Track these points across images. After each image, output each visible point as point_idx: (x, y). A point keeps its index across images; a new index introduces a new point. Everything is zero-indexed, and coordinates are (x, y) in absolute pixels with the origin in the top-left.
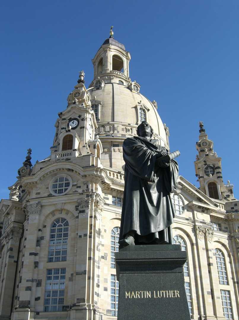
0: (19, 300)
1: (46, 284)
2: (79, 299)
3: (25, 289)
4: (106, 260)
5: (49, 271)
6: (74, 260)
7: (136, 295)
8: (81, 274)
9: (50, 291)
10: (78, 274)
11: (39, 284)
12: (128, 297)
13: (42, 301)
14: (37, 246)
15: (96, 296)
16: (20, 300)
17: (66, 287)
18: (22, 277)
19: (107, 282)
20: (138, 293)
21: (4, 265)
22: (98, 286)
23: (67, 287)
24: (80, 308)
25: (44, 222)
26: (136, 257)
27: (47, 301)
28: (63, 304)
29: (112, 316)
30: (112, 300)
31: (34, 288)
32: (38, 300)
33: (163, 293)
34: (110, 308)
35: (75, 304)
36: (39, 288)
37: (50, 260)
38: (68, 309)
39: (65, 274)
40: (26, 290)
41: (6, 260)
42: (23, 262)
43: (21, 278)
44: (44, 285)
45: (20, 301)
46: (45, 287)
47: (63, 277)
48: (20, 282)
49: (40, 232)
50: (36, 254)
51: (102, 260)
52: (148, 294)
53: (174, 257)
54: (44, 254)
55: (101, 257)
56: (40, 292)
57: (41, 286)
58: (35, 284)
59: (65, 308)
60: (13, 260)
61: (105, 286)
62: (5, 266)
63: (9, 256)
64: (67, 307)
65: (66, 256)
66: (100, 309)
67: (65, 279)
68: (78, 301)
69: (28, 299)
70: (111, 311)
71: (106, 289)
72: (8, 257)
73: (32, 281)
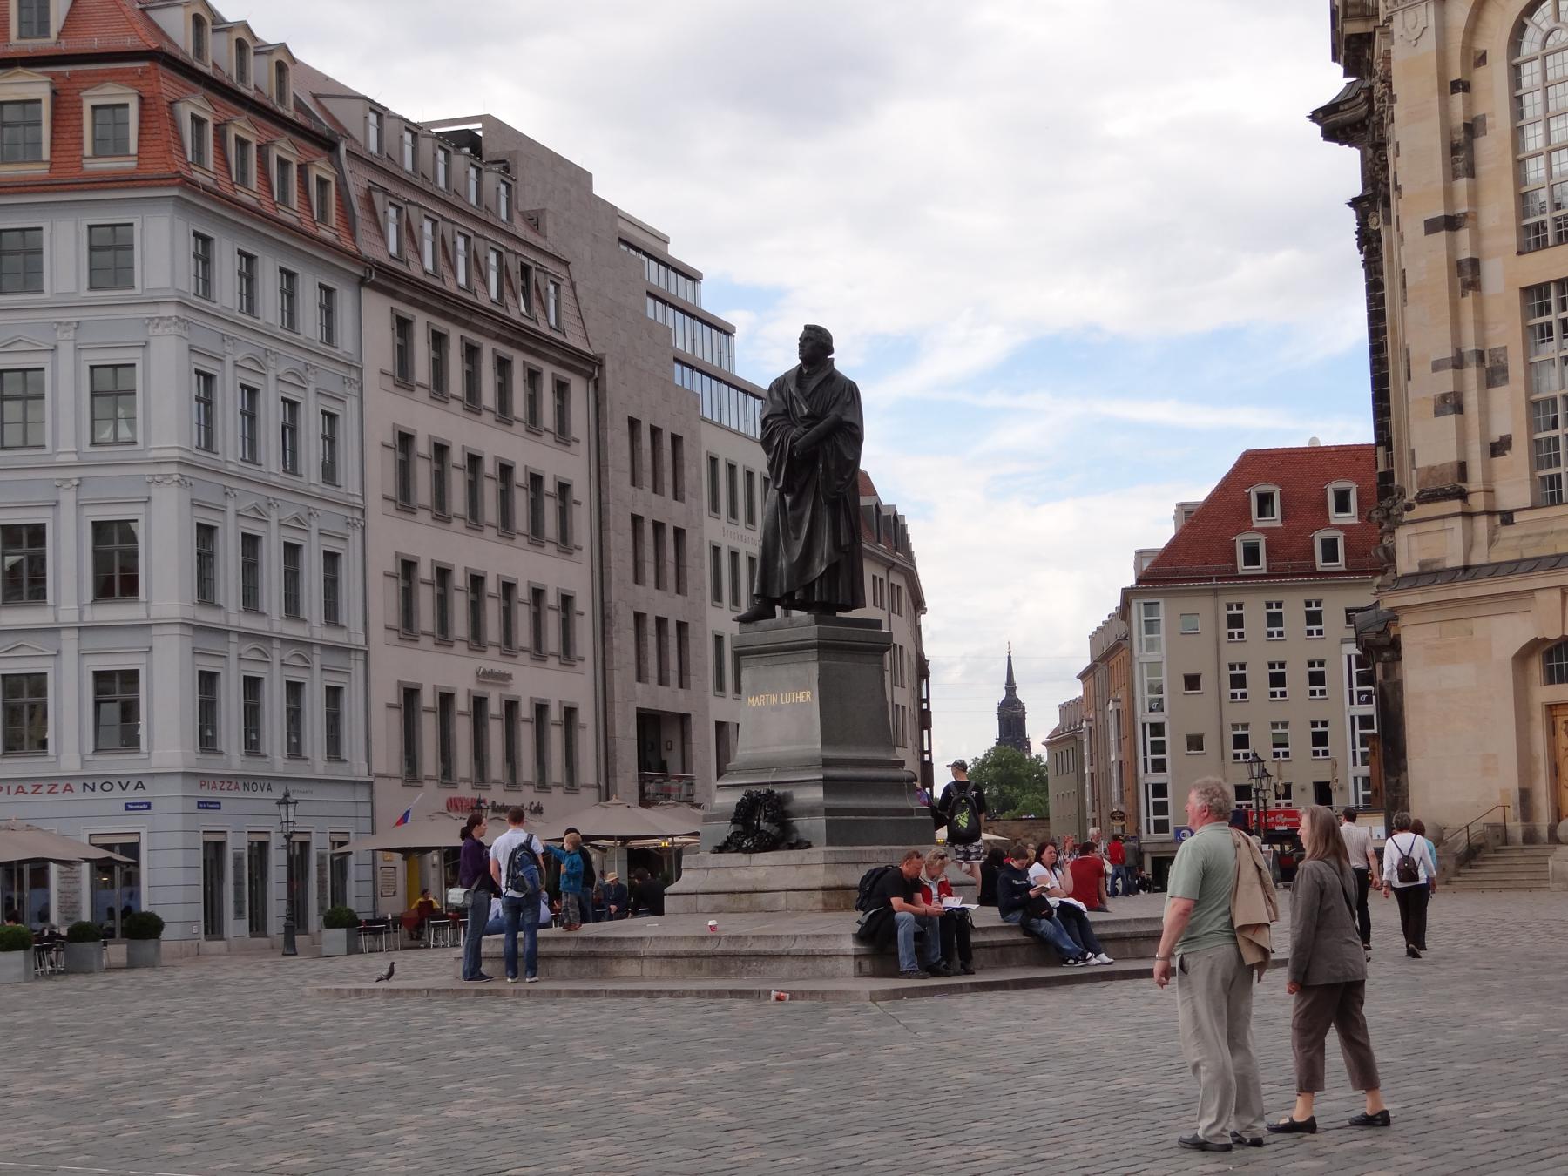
1: (1530, 367)
5: (1535, 295)
9: (1554, 400)
11: (1494, 375)
13: (1520, 453)
14: (1455, 177)
25: (1472, 30)
27: (1545, 453)
31: (1472, 400)
32: (1503, 454)
36: (1499, 395)
37: (1532, 239)
40: (1437, 414)
44: (1521, 372)
45: (1418, 471)
46: (1531, 386)
49: (1459, 96)
50: (1451, 223)
52: (774, 698)
54: (1497, 213)
56: (1506, 411)
57: (1506, 378)
58: (1472, 374)
69: (1452, 457)
73: (1458, 362)
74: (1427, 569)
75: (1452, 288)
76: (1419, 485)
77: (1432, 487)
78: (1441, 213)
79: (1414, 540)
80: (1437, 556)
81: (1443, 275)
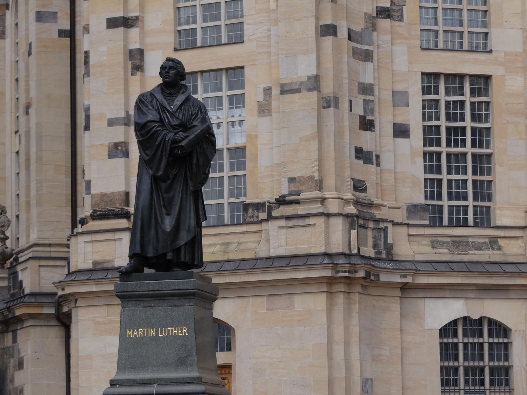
0: (90, 193)
2: (295, 179)
3: (106, 153)
4: (401, 19)
6: (269, 37)
7: (139, 333)
8: (298, 91)
10: (286, 90)
12: (130, 335)
15: (361, 162)
16: (94, 191)
17: (249, 137)
18: (92, 112)
19: (407, 105)
20: (141, 331)
21: (23, 48)
22: (367, 125)
23: (252, 138)
24: (300, 210)
26: (139, 289)
28: (245, 195)
29: (433, 225)
30: (429, 169)
33: (169, 330)
34: (420, 199)
35: (284, 196)
38: (263, 216)
39: (243, 88)
40: (111, 156)
41: (27, 29)
42: (87, 53)
43: (87, 110)
45: (93, 196)
47: (236, 101)
48: (87, 128)
50: (126, 23)
51: (384, 23)
52: (152, 332)
53: (182, 287)
55: (375, 15)
59: (250, 212)
60: (52, 29)
61: (400, 120)
62: (30, 54)
63: (38, 13)
64: (259, 206)
65: (242, 23)
66: (379, 206)
67: (244, 107)
68: (292, 184)
69: (122, 188)
70: (424, 208)
71: (401, 131)
72: (32, 16)
74: (99, 267)
75: (125, 68)
76: (93, 206)
77: (104, 208)
78: (120, 14)
79: (90, 245)
80: (107, 258)
81: (121, 58)
